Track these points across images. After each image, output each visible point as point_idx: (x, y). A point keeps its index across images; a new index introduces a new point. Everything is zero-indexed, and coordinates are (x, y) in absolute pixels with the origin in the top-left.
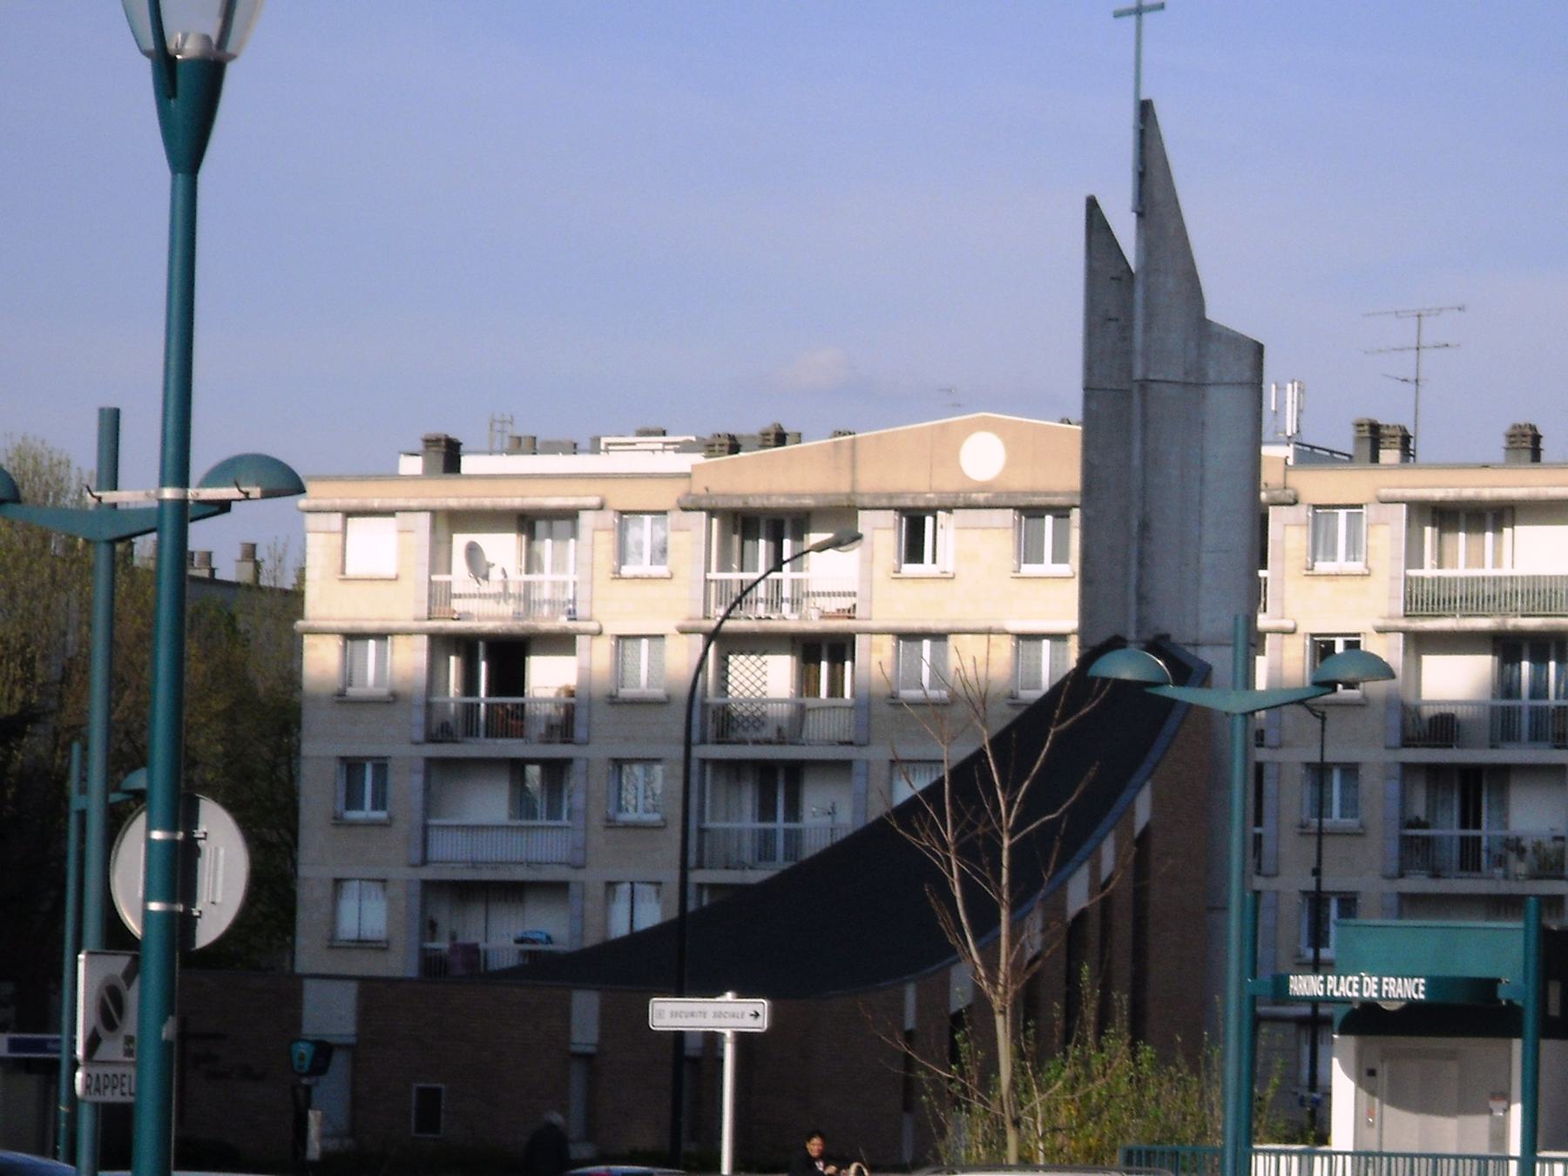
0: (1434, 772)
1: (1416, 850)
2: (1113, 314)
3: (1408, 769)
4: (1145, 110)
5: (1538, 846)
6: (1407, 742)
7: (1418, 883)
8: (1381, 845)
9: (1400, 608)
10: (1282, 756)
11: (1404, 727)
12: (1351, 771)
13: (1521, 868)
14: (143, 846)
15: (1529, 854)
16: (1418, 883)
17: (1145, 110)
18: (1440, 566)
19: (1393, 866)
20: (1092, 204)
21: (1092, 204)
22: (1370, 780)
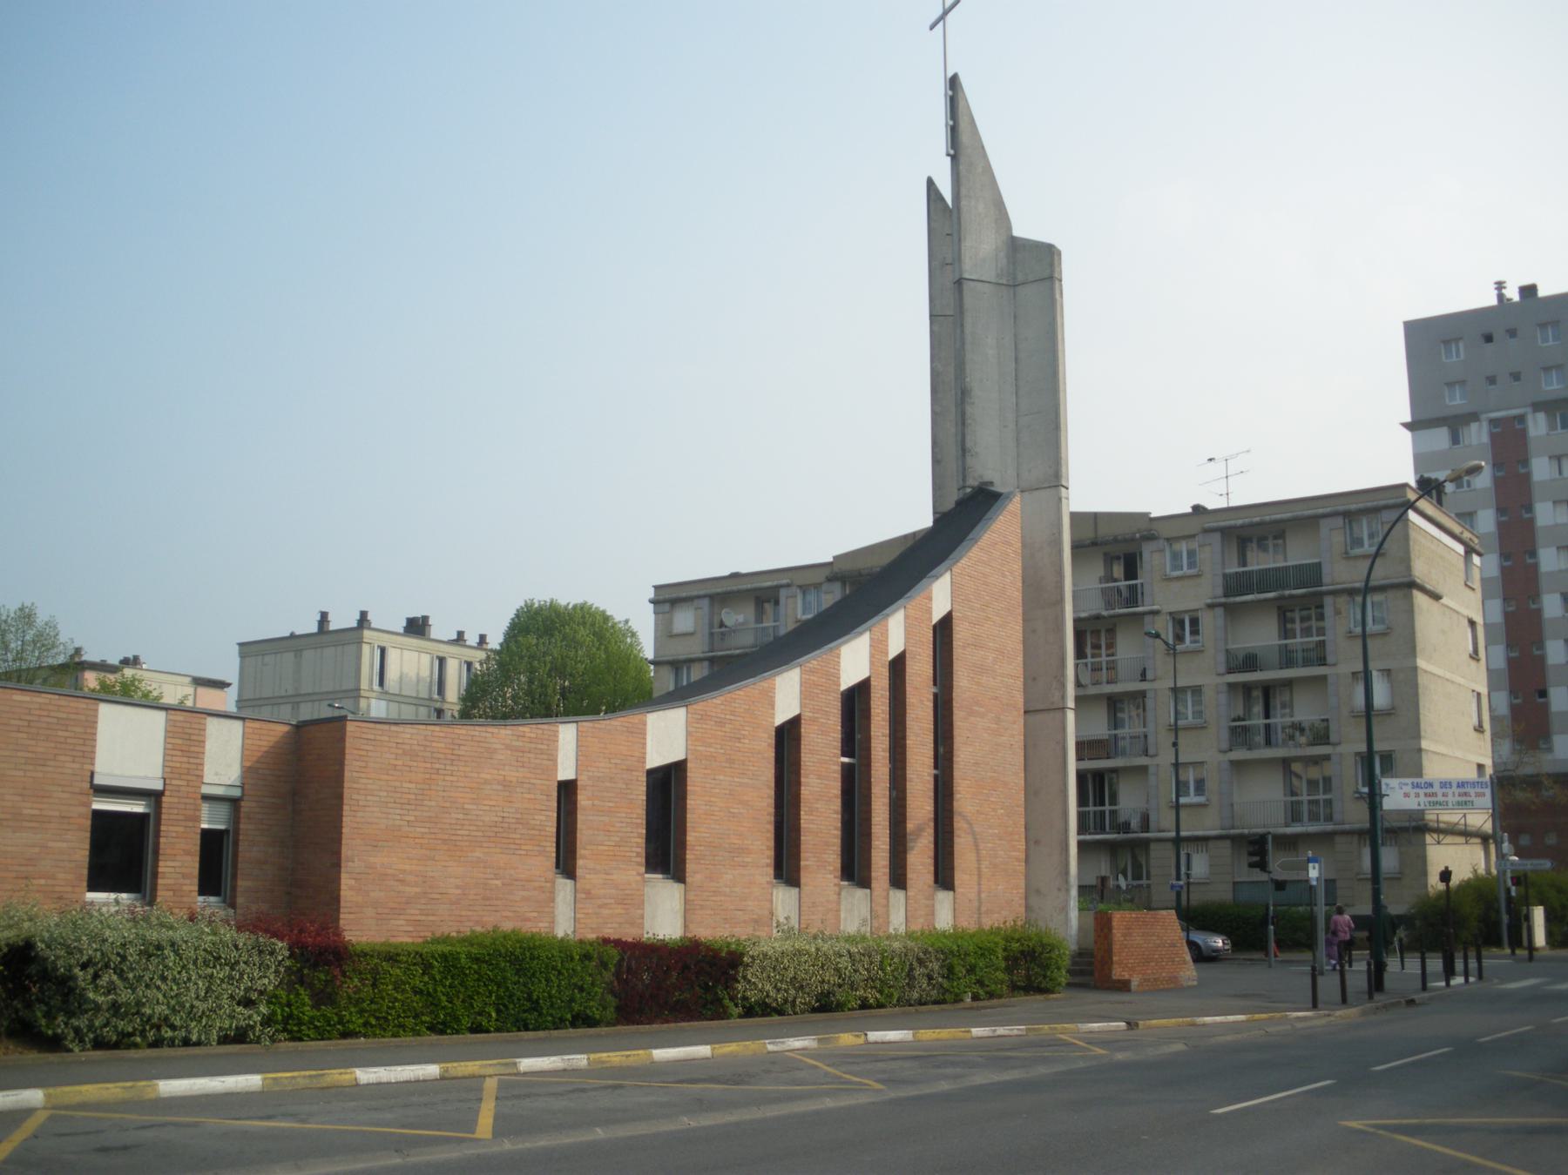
0: (1247, 688)
1: (1240, 735)
2: (949, 261)
3: (1232, 686)
4: (954, 83)
5: (1312, 727)
6: (1230, 671)
7: (1240, 754)
8: (1218, 732)
9: (1220, 591)
10: (1156, 685)
11: (1228, 662)
12: (1197, 690)
13: (1303, 740)
14: (1186, 949)
15: (1307, 732)
16: (1240, 754)
17: (954, 83)
18: (1245, 565)
19: (1225, 746)
20: (930, 182)
21: (930, 182)
22: (1208, 694)
